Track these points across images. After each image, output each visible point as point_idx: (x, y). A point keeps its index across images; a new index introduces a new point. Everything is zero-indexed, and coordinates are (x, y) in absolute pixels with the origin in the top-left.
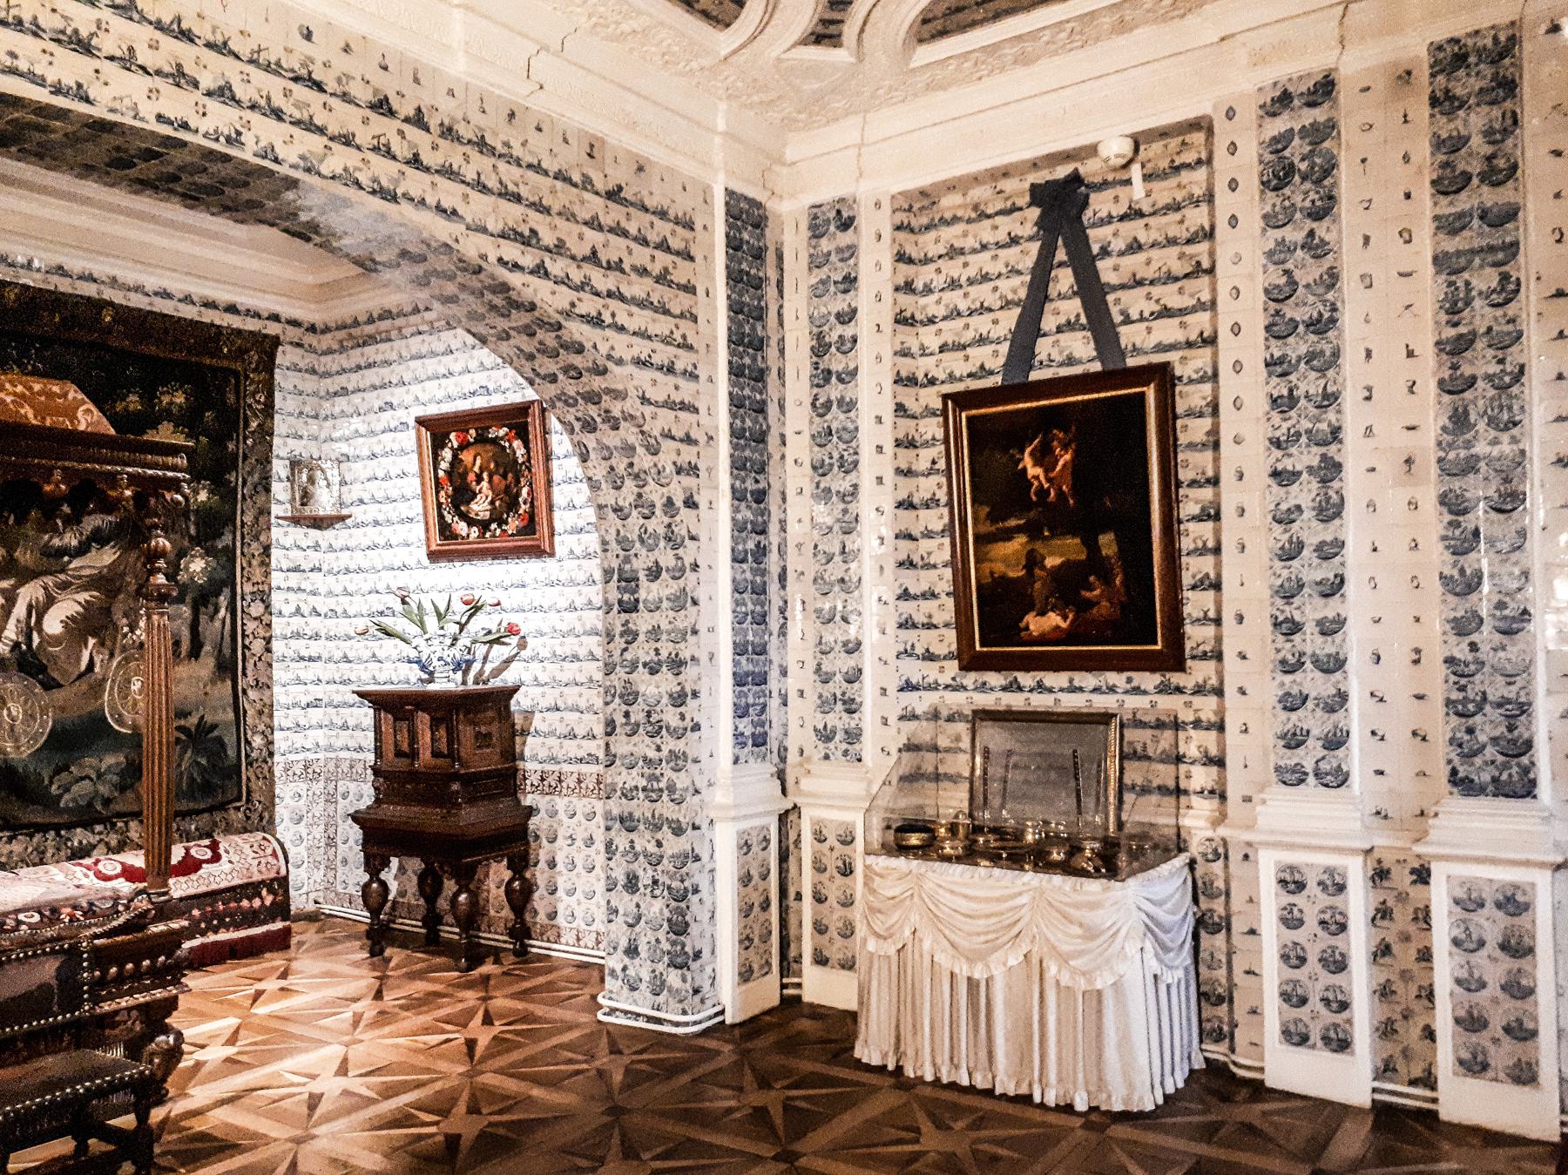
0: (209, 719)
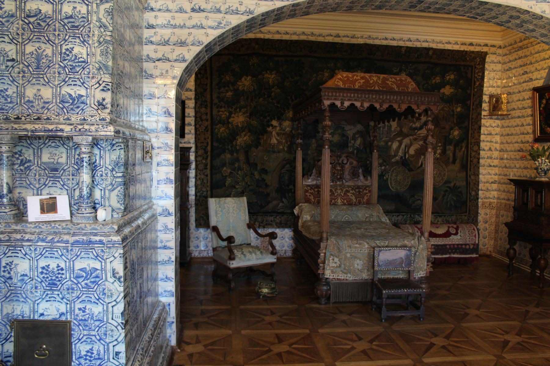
0: (457, 184)
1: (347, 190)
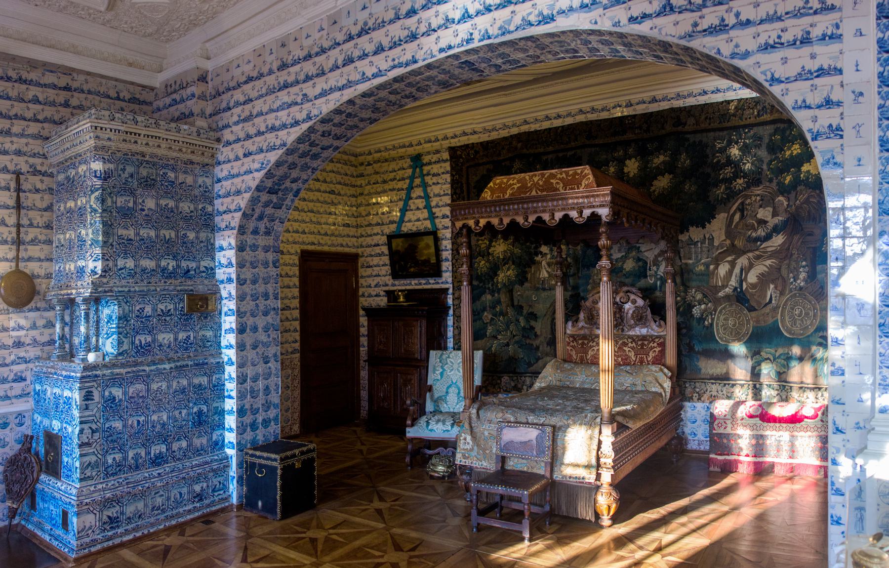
1: (624, 342)
